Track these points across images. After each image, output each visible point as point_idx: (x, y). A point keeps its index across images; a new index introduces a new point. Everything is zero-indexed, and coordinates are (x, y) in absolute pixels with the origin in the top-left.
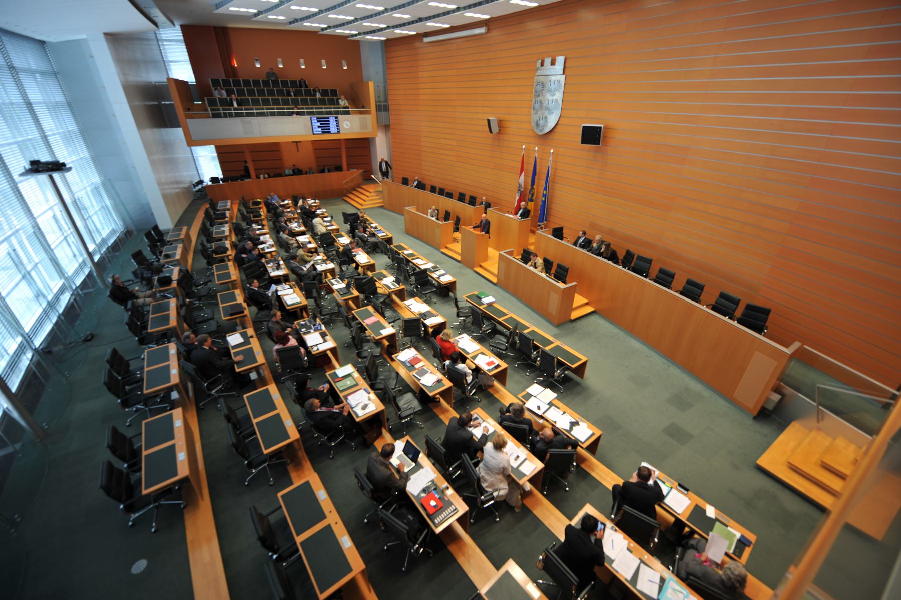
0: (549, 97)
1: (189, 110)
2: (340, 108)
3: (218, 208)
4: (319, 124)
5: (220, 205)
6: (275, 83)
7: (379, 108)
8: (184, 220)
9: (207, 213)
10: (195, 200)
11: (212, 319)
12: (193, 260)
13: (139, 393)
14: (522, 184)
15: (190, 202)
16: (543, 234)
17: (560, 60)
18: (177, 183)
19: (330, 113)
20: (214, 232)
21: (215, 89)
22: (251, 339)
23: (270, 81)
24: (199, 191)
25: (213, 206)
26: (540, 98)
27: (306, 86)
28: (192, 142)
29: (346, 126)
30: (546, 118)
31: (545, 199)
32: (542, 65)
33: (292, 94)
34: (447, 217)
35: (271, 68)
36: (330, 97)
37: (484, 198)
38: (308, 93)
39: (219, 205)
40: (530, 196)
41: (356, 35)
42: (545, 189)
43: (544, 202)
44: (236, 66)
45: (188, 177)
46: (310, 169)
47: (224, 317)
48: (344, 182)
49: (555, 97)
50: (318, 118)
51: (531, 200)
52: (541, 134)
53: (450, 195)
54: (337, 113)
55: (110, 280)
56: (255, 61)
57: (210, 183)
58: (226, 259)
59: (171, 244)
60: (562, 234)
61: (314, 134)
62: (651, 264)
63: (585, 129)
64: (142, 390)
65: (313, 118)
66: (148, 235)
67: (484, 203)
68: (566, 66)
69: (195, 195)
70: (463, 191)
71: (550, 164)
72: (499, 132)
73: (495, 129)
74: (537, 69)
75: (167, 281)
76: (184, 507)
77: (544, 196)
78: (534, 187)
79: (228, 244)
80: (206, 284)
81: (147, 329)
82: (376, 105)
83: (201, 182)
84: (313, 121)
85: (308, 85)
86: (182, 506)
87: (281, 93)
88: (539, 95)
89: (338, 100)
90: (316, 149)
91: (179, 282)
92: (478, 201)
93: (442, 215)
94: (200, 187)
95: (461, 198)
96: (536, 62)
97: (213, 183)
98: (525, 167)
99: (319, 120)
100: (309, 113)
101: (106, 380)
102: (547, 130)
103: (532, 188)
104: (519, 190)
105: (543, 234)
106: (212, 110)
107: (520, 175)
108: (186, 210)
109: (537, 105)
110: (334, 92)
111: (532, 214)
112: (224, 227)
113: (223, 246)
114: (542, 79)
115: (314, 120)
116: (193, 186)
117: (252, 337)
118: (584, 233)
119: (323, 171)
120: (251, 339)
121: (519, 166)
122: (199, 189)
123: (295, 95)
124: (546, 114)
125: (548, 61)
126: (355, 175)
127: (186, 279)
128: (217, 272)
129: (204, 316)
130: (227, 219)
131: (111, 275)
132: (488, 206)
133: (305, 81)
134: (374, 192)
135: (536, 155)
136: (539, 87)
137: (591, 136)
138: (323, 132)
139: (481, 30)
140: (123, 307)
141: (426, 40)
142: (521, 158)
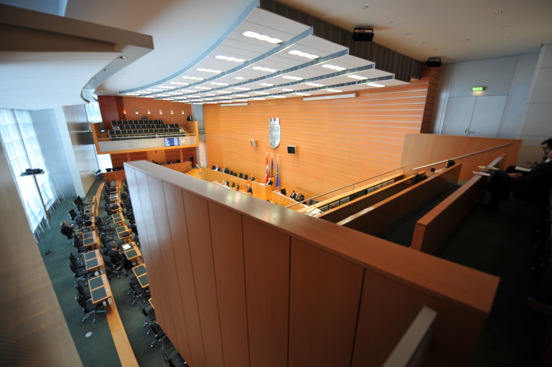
0: (274, 133)
1: (100, 137)
2: (179, 134)
3: (112, 185)
5: (112, 184)
6: (146, 122)
7: (200, 133)
8: (91, 192)
9: (105, 187)
10: (95, 181)
11: (113, 240)
12: (99, 213)
13: (84, 270)
14: (268, 169)
15: (93, 181)
16: (276, 192)
17: (277, 119)
18: (87, 171)
20: (110, 199)
21: (114, 126)
22: (134, 247)
23: (143, 121)
24: (99, 176)
25: (108, 184)
26: (272, 133)
27: (162, 123)
28: (99, 152)
29: (183, 142)
30: (274, 142)
32: (271, 120)
33: (156, 127)
34: (234, 186)
35: (144, 115)
36: (175, 128)
37: (252, 176)
38: (163, 126)
39: (112, 183)
40: (272, 175)
41: (188, 103)
42: (277, 172)
43: (277, 177)
45: (93, 169)
46: (163, 162)
47: (120, 237)
48: (181, 168)
49: (277, 134)
51: (272, 177)
52: (273, 148)
53: (235, 175)
54: (178, 136)
55: (61, 224)
56: (136, 112)
57: (106, 172)
58: (117, 212)
59: (87, 206)
60: (285, 192)
61: (166, 146)
63: (289, 148)
64: (85, 269)
65: (165, 139)
66: (76, 202)
67: (251, 178)
68: (280, 121)
69: (96, 178)
70: (242, 172)
71: (278, 161)
72: (257, 146)
73: (254, 145)
74: (269, 122)
75: (90, 223)
76: (107, 313)
77: (277, 175)
78: (273, 170)
79: (119, 204)
80: (108, 224)
81: (83, 245)
82: (199, 132)
83: (99, 171)
84: (165, 140)
85: (164, 122)
86: (105, 313)
87: (149, 127)
88: (271, 132)
89: (179, 129)
90: (166, 152)
91: (96, 224)
92: (248, 178)
93: (231, 184)
94: (99, 173)
95: (241, 176)
96: (268, 119)
97: (107, 171)
98: (268, 162)
100: (163, 137)
101: (71, 264)
102: (276, 146)
104: (267, 172)
105: (276, 192)
106: (112, 137)
108: (92, 186)
109: (270, 136)
110: (177, 126)
111: (273, 183)
112: (115, 195)
113: (116, 205)
114: (271, 126)
115: (166, 139)
116: (95, 174)
117: (134, 245)
118: (294, 192)
119: (169, 163)
120: (134, 247)
121: (266, 163)
122: (99, 175)
123: (157, 128)
124: (274, 140)
125: (273, 119)
126: (188, 164)
127: (99, 222)
128: (114, 218)
129: (109, 238)
130: (117, 191)
131: (62, 222)
132: (253, 179)
133: (162, 121)
134: (198, 173)
135: (272, 157)
136: (271, 129)
137: (291, 150)
140: (67, 237)
141: (222, 105)
142: (266, 158)
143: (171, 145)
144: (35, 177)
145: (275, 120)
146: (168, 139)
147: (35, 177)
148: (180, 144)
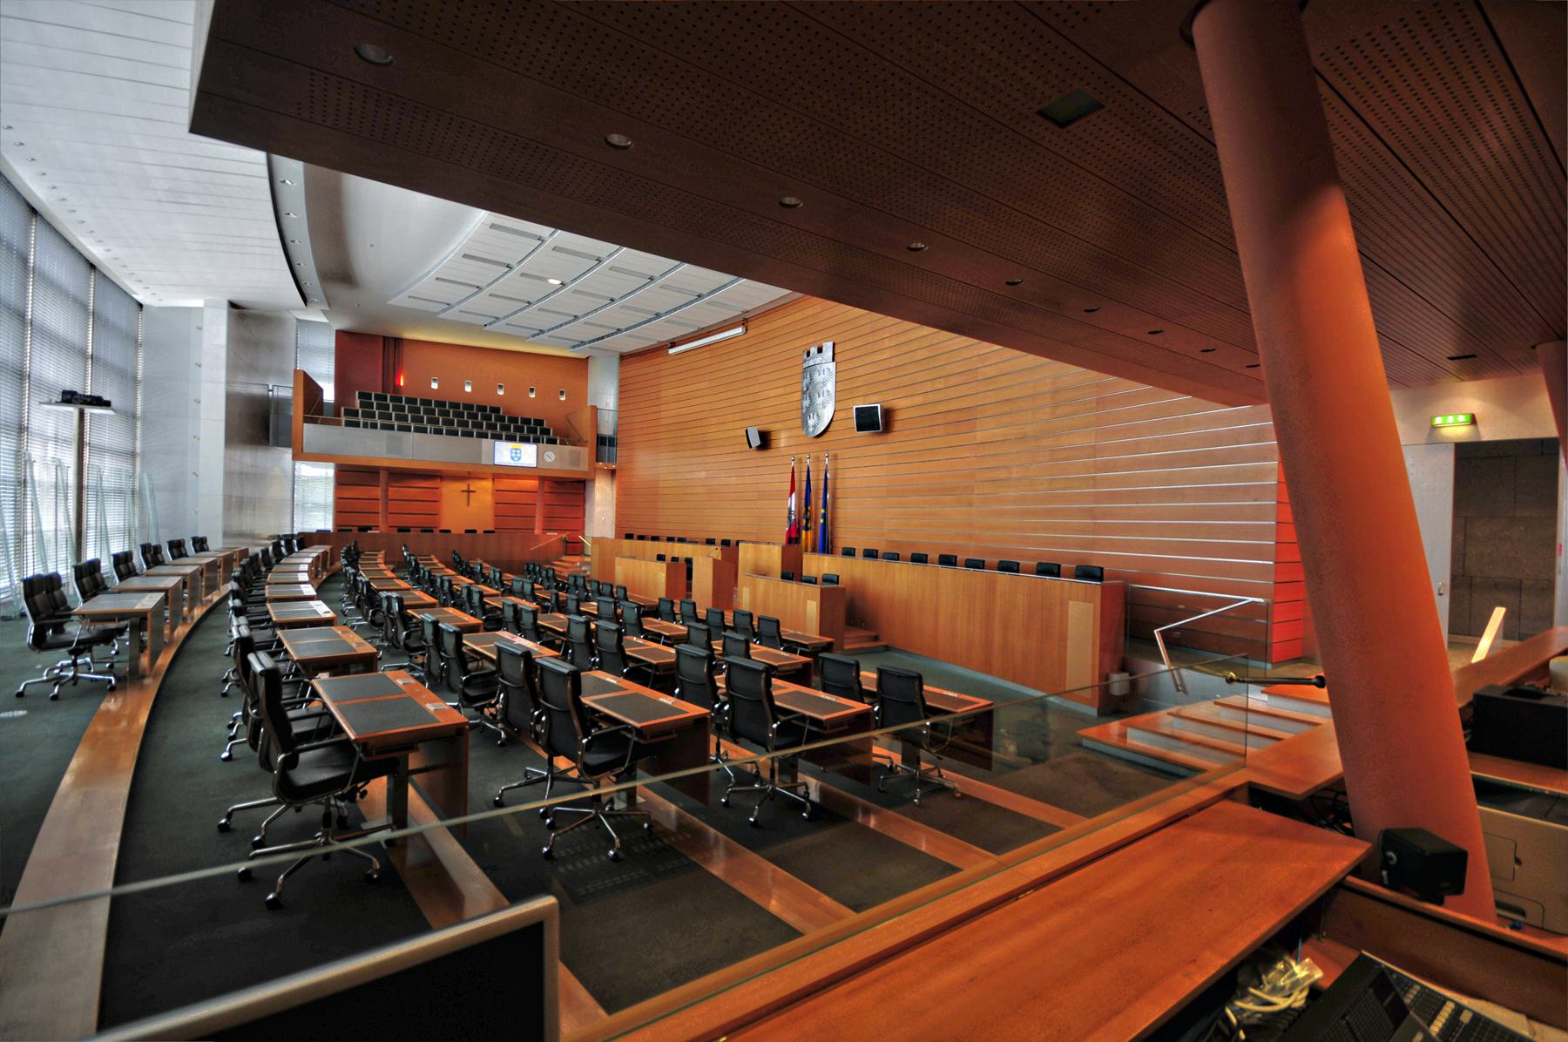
31: (825, 520)
40: (804, 521)
43: (824, 524)
44: (402, 384)
73: (756, 441)
103: (807, 510)
104: (789, 518)
107: (791, 495)
121: (788, 486)
125: (814, 350)
139: (739, 330)
144: (82, 415)
145: (820, 350)
147: (82, 415)
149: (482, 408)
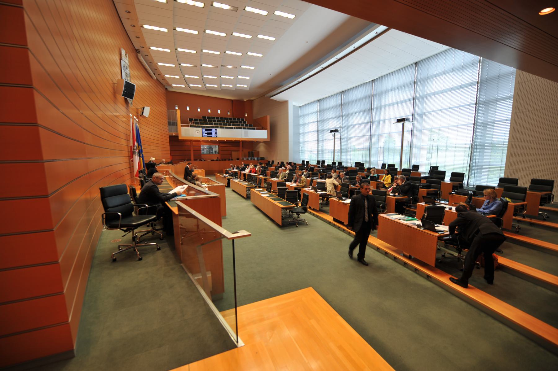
4: (206, 132)
19: (214, 127)
50: (206, 129)
62: (271, 185)
65: (203, 129)
84: (203, 131)
99: (206, 130)
100: (201, 127)
115: (204, 130)
138: (208, 136)
143: (208, 136)
146: (206, 129)
148: (218, 136)
149: (213, 118)
